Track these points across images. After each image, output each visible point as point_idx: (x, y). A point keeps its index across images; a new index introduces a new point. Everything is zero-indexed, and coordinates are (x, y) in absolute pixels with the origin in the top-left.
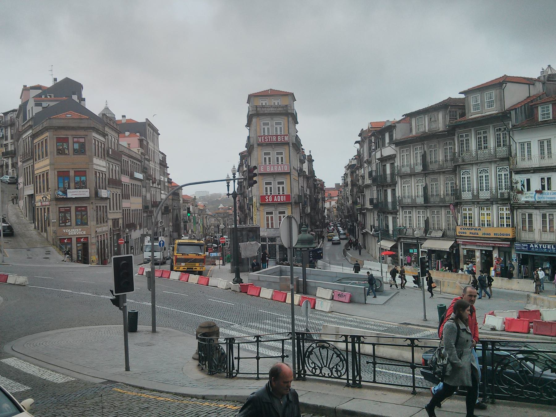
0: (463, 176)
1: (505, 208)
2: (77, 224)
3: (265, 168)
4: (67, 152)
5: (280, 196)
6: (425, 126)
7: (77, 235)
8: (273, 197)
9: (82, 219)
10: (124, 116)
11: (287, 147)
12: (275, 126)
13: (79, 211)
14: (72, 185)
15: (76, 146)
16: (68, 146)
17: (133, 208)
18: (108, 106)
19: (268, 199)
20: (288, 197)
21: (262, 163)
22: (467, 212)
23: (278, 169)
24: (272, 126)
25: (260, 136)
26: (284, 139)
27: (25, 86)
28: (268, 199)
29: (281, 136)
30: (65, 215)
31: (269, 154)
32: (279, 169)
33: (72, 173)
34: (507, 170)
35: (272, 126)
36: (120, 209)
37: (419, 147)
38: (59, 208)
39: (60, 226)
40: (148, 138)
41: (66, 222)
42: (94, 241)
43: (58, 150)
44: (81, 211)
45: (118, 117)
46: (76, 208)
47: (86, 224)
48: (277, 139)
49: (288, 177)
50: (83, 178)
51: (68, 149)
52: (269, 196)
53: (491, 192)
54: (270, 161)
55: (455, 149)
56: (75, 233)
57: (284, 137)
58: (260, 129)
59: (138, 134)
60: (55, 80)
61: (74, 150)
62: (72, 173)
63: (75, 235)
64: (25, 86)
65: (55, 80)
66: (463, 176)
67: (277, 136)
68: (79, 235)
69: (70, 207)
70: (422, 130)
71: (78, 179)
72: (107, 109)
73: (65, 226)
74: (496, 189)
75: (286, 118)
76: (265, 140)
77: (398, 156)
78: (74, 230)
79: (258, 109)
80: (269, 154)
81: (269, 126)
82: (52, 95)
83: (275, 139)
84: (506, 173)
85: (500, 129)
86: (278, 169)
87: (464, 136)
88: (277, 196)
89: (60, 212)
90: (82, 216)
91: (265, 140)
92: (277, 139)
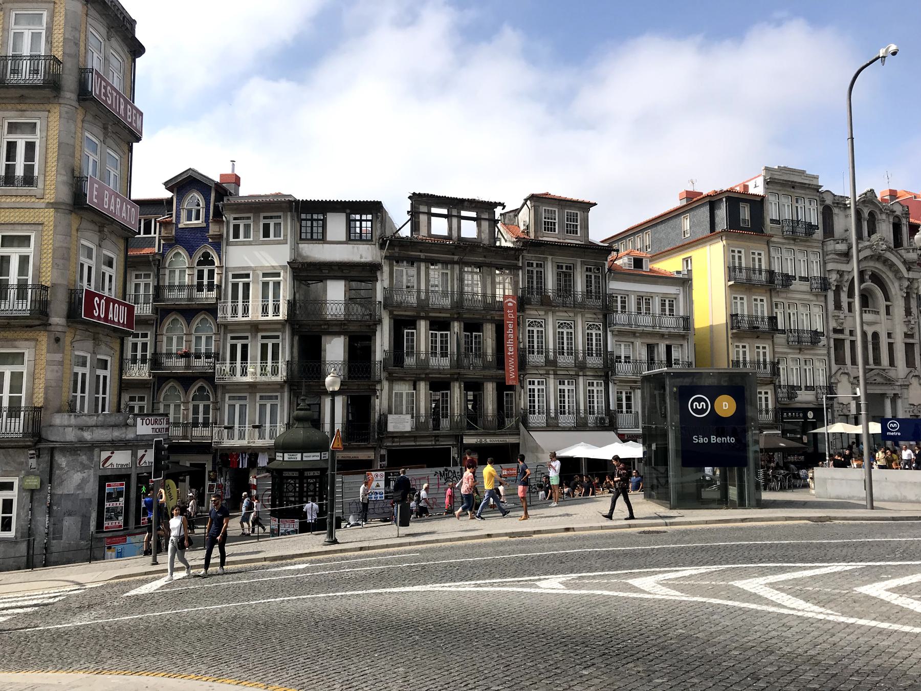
0: (531, 329)
22: (536, 387)
66: (531, 329)
77: (386, 269)
84: (598, 332)
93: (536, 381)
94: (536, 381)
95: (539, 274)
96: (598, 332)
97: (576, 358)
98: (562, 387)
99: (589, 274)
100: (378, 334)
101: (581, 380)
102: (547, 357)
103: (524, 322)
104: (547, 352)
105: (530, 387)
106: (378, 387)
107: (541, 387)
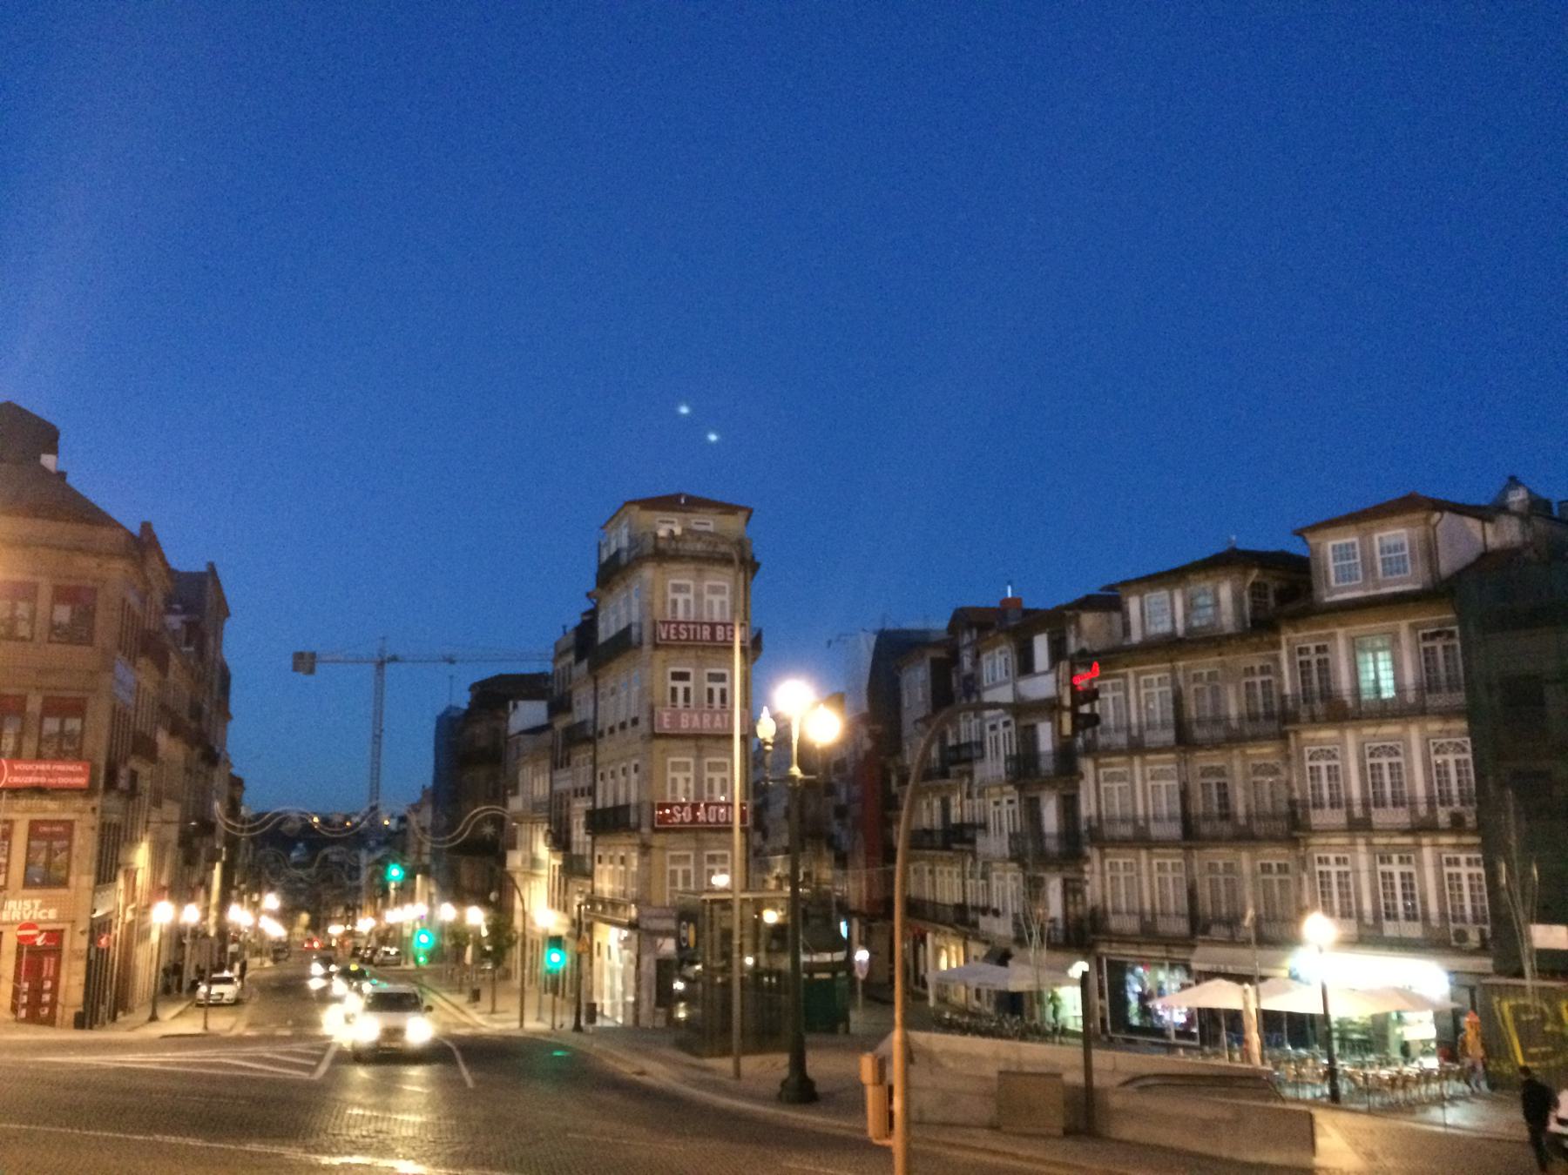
0: (1314, 764)
1: (1463, 857)
2: (28, 883)
3: (675, 719)
6: (1173, 622)
9: (48, 864)
13: (43, 836)
14: (30, 746)
15: (63, 614)
21: (664, 704)
22: (1333, 869)
23: (712, 722)
24: (699, 596)
25: (664, 623)
29: (724, 625)
31: (683, 676)
32: (718, 724)
33: (34, 704)
34: (1464, 750)
35: (699, 596)
37: (1155, 677)
42: (82, 943)
44: (52, 836)
46: (34, 826)
47: (63, 883)
48: (713, 634)
50: (73, 724)
53: (1414, 811)
54: (687, 698)
55: (1281, 687)
58: (664, 603)
61: (54, 627)
62: (34, 704)
66: (1314, 764)
67: (713, 626)
70: (1163, 627)
71: (52, 725)
74: (1430, 802)
76: (677, 633)
80: (683, 676)
83: (706, 633)
84: (1461, 757)
85: (1438, 634)
86: (712, 722)
87: (1313, 651)
90: (51, 853)
91: (677, 633)
92: (713, 634)
93: (1332, 857)
94: (1332, 857)
95: (1324, 665)
96: (1461, 757)
97: (1414, 811)
98: (1386, 868)
99: (1428, 644)
100: (1082, 793)
101: (1427, 854)
102: (1350, 814)
103: (1300, 752)
104: (1349, 803)
105: (1318, 868)
106: (1087, 868)
107: (1343, 868)
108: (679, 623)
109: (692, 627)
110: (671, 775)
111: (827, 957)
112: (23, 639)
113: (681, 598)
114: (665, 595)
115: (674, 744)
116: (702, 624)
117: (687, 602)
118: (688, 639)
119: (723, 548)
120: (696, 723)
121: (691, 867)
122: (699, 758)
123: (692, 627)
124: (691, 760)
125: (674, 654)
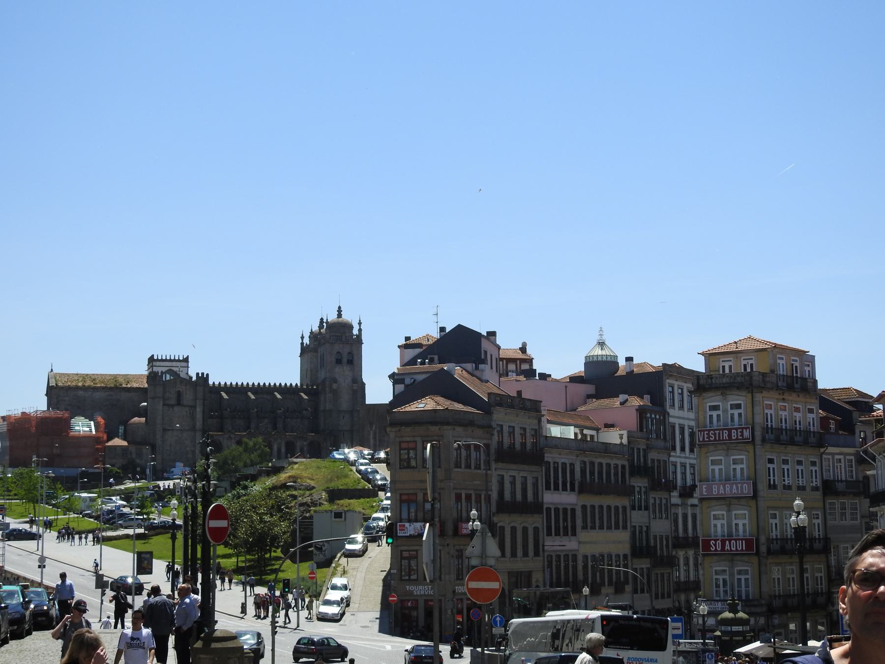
3: (710, 489)
4: (413, 463)
5: (736, 540)
7: (425, 595)
8: (723, 542)
10: (629, 359)
11: (750, 448)
12: (730, 412)
16: (416, 455)
17: (588, 550)
18: (604, 337)
19: (715, 545)
20: (749, 542)
24: (725, 411)
25: (700, 431)
26: (742, 435)
27: (407, 339)
28: (715, 545)
29: (736, 429)
30: (409, 563)
31: (719, 462)
35: (725, 411)
36: (537, 554)
38: (402, 551)
39: (401, 580)
40: (668, 404)
41: (410, 575)
43: (401, 460)
45: (622, 362)
48: (730, 435)
49: (752, 503)
51: (416, 458)
52: (716, 540)
56: (422, 592)
57: (742, 432)
58: (705, 418)
59: (647, 397)
60: (442, 329)
63: (422, 595)
64: (407, 339)
65: (442, 329)
67: (730, 430)
68: (428, 595)
69: (417, 551)
72: (602, 344)
73: (409, 580)
75: (750, 395)
76: (709, 437)
78: (421, 587)
79: (702, 382)
81: (720, 412)
82: (436, 357)
83: (726, 435)
88: (730, 541)
89: (402, 558)
91: (709, 437)
92: (730, 435)
108: (709, 431)
109: (717, 432)
110: (713, 522)
111: (729, 628)
112: (413, 468)
113: (715, 414)
114: (705, 412)
115: (714, 503)
116: (723, 430)
117: (718, 416)
118: (715, 440)
119: (739, 379)
120: (722, 491)
121: (727, 577)
122: (729, 511)
123: (717, 432)
124: (724, 513)
125: (711, 448)
